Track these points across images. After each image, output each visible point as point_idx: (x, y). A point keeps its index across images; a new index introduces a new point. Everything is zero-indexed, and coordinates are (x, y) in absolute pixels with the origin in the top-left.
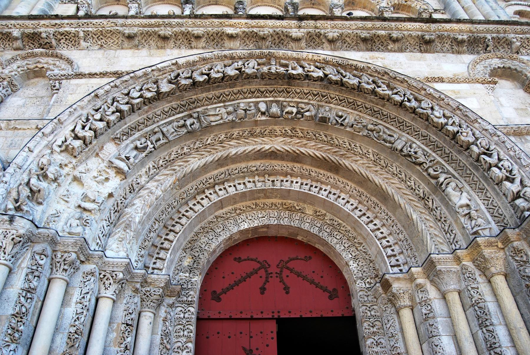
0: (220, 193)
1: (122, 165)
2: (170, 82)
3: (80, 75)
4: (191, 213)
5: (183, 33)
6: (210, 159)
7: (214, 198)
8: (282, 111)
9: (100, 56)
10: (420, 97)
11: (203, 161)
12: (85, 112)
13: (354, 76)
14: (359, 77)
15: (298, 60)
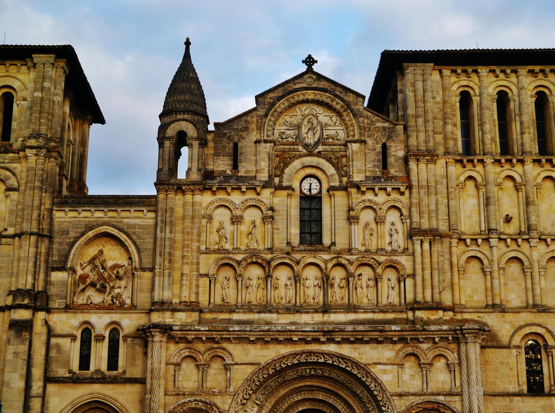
0: (292, 400)
1: (258, 402)
2: (272, 369)
3: (237, 364)
4: (281, 409)
5: (275, 339)
6: (287, 390)
7: (290, 403)
8: (315, 372)
9: (241, 348)
10: (368, 375)
11: (285, 391)
12: (244, 387)
13: (345, 362)
14: (346, 363)
15: (323, 354)
